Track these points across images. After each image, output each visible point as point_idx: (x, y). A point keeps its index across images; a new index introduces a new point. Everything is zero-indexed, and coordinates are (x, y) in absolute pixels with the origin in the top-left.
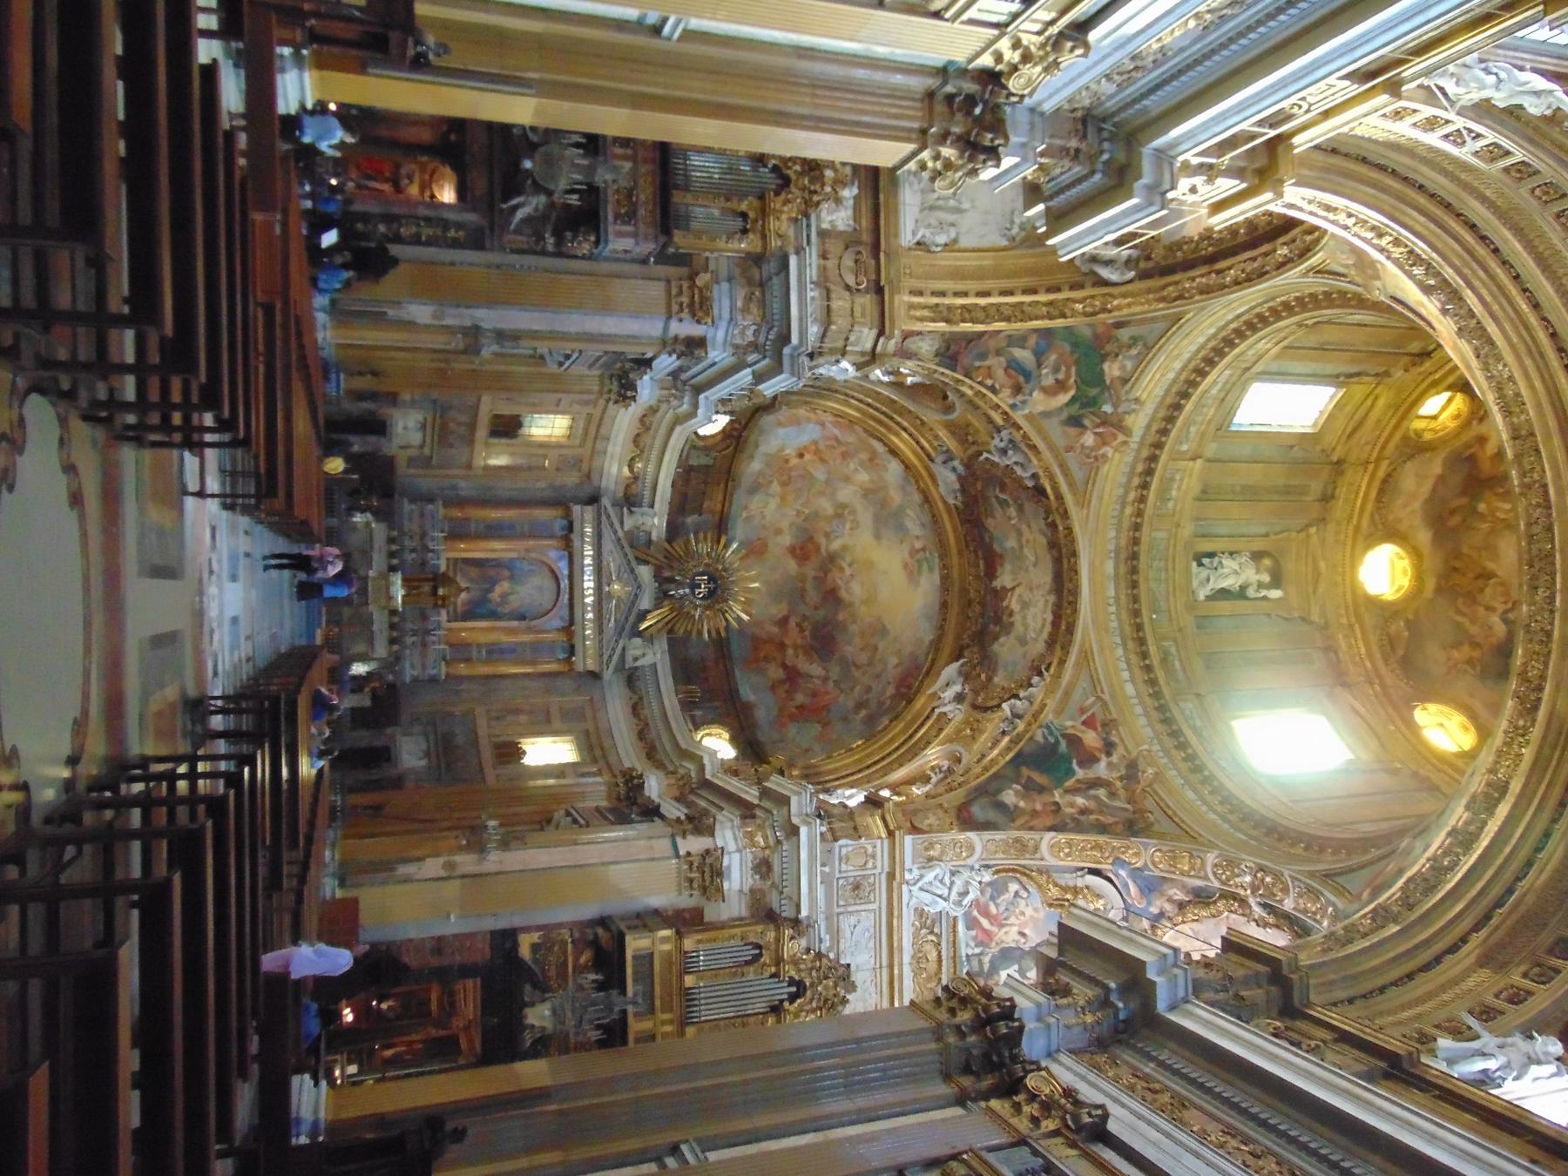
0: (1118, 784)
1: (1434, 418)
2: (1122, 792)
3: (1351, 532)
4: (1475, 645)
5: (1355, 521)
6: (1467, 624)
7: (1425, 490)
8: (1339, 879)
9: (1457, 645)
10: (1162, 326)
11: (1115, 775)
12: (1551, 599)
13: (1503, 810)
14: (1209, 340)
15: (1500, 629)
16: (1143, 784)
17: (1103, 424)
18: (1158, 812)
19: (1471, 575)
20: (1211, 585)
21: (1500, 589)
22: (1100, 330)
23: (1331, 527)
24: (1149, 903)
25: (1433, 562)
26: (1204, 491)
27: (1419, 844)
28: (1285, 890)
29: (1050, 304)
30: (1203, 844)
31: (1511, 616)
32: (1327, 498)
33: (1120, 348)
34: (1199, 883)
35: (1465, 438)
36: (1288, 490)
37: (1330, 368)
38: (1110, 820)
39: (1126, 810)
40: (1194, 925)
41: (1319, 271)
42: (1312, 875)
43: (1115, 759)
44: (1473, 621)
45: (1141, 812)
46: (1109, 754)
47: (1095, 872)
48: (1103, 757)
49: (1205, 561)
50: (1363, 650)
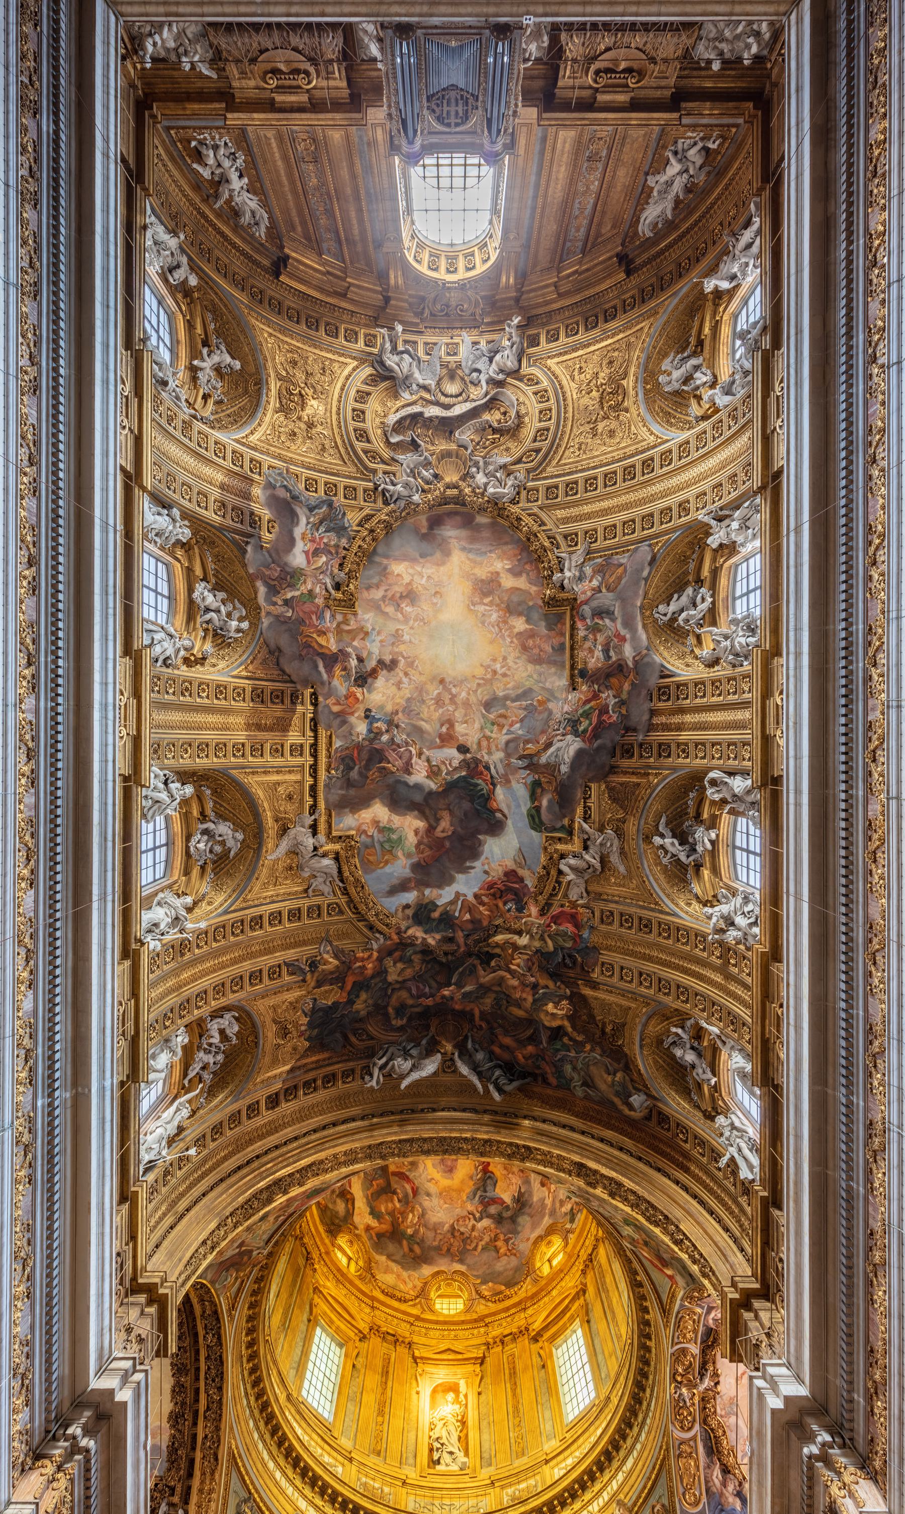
1: (350, 1259)
4: (496, 1238)
5: (412, 1320)
8: (664, 1298)
9: (497, 1250)
12: (466, 1139)
15: (486, 1222)
18: (652, 1501)
20: (455, 1450)
23: (416, 1339)
25: (443, 1265)
26: (379, 1454)
27: (627, 1231)
28: (684, 1351)
30: (668, 1444)
32: (396, 1340)
35: (365, 1238)
36: (385, 1373)
37: (303, 1327)
40: (739, 1456)
41: (232, 1307)
42: (666, 1326)
49: (436, 1456)
50: (504, 1315)
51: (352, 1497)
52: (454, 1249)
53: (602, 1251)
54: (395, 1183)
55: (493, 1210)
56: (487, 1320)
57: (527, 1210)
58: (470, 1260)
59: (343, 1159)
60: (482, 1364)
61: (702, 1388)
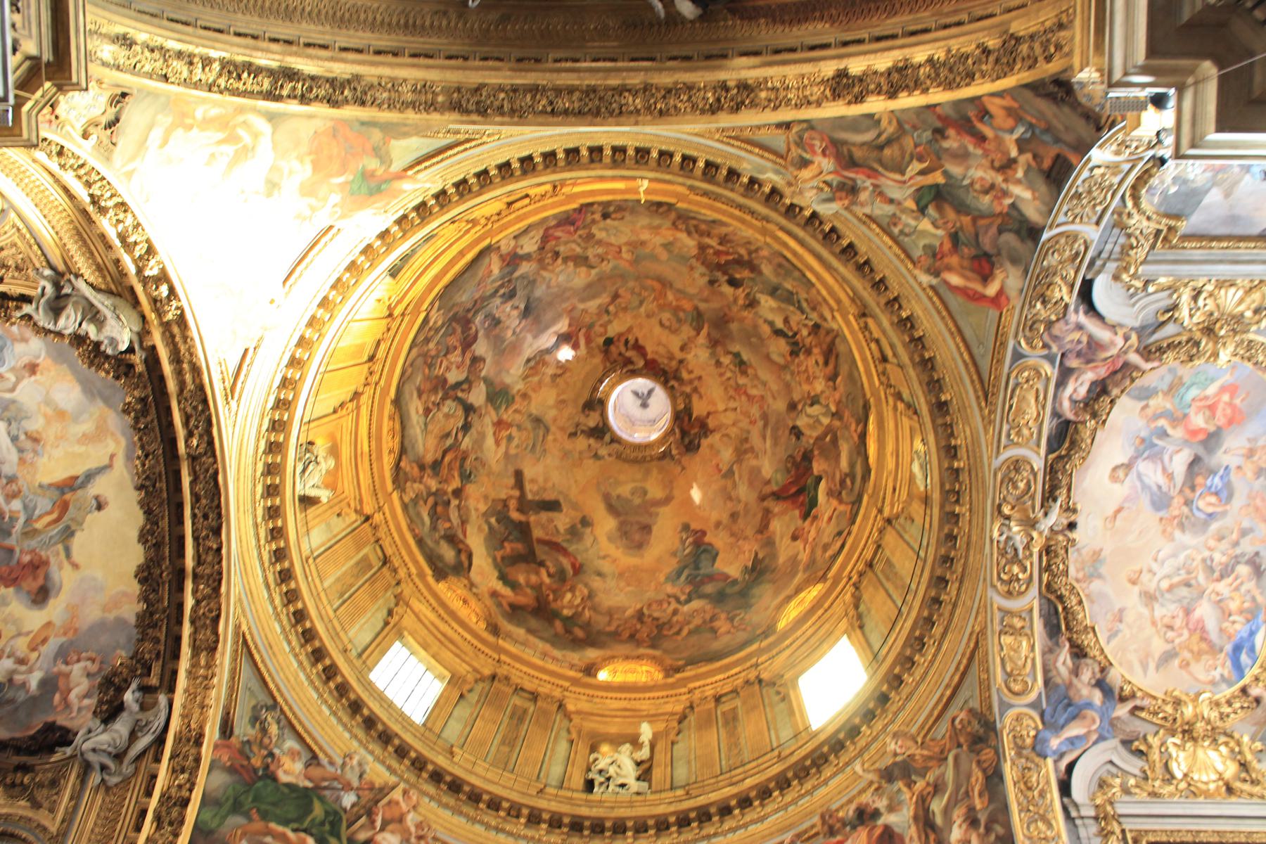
0: (920, 785)
2: (931, 777)
3: (578, 690)
4: (713, 619)
5: (566, 684)
6: (692, 626)
7: (541, 645)
8: (985, 364)
9: (714, 631)
10: (246, 671)
11: (906, 795)
12: (634, 92)
13: (856, 66)
14: (289, 643)
15: (696, 604)
16: (914, 750)
17: (370, 813)
19: (639, 626)
21: (654, 606)
22: (225, 758)
24: (1089, 705)
29: (158, 818)
31: (683, 598)
32: (534, 696)
33: (261, 745)
34: (1038, 625)
36: (519, 717)
38: (978, 775)
39: (956, 758)
42: (988, 422)
43: (881, 804)
44: (689, 623)
45: (955, 733)
46: (876, 814)
47: (1065, 788)
48: (881, 822)
51: (450, 769)
52: (644, 633)
53: (890, 538)
54: (541, 552)
55: (709, 588)
56: (692, 685)
57: (768, 576)
58: (667, 644)
59: (409, 97)
60: (680, 722)
61: (1046, 525)
